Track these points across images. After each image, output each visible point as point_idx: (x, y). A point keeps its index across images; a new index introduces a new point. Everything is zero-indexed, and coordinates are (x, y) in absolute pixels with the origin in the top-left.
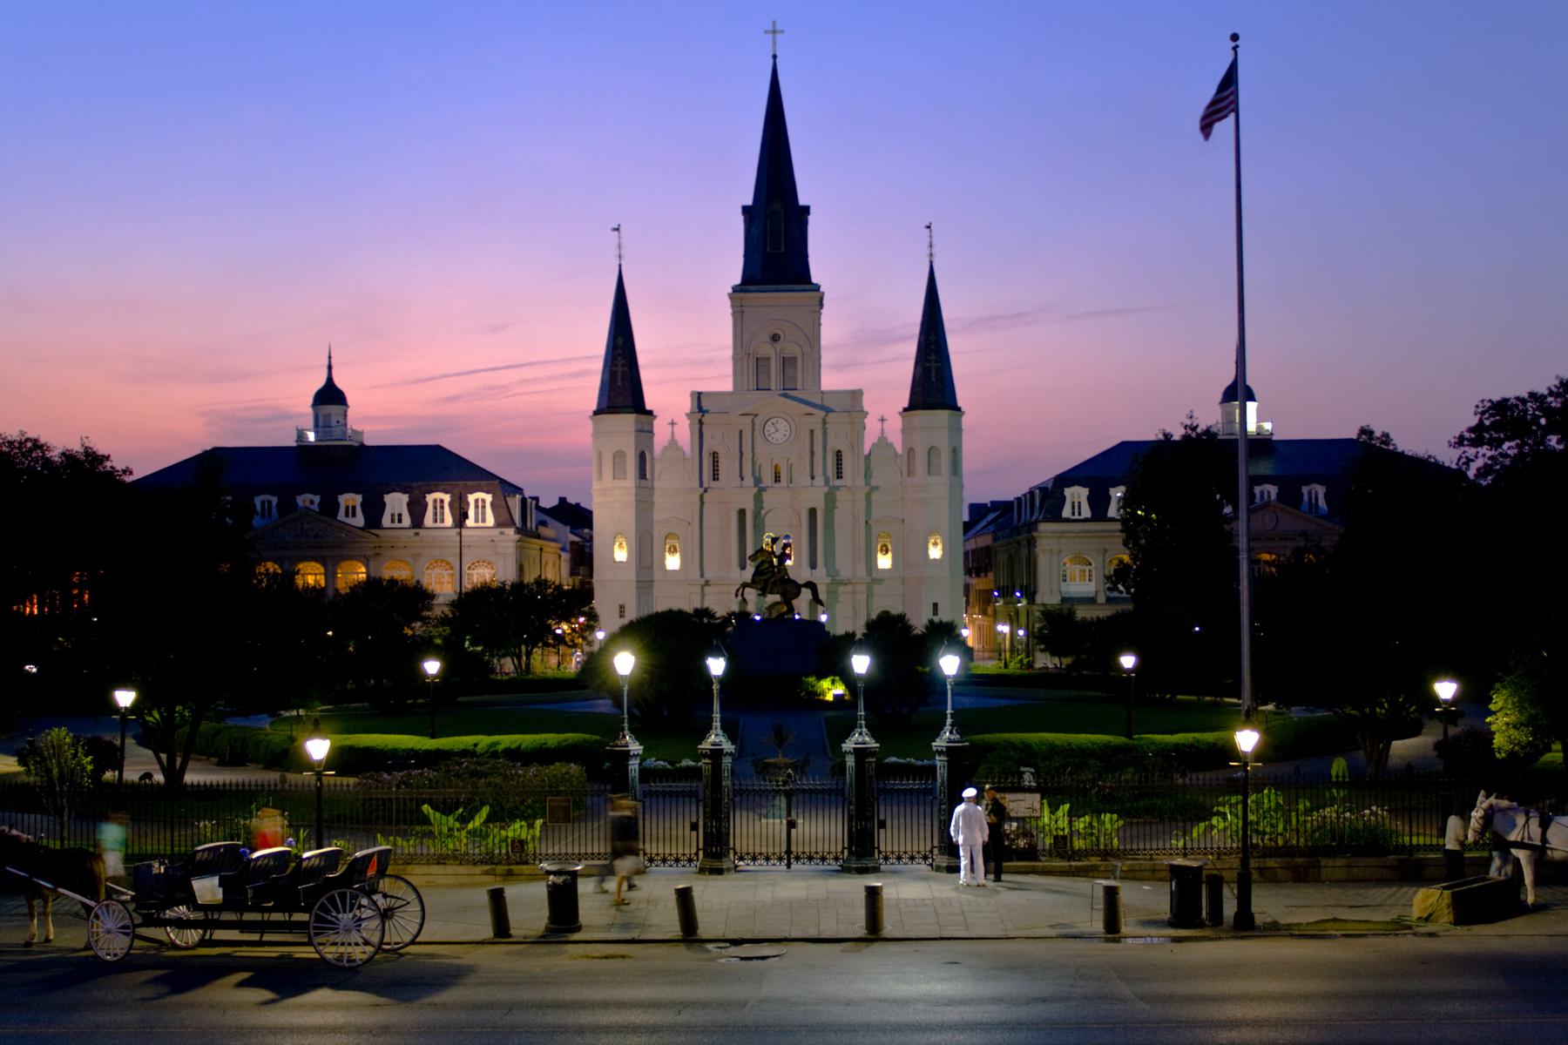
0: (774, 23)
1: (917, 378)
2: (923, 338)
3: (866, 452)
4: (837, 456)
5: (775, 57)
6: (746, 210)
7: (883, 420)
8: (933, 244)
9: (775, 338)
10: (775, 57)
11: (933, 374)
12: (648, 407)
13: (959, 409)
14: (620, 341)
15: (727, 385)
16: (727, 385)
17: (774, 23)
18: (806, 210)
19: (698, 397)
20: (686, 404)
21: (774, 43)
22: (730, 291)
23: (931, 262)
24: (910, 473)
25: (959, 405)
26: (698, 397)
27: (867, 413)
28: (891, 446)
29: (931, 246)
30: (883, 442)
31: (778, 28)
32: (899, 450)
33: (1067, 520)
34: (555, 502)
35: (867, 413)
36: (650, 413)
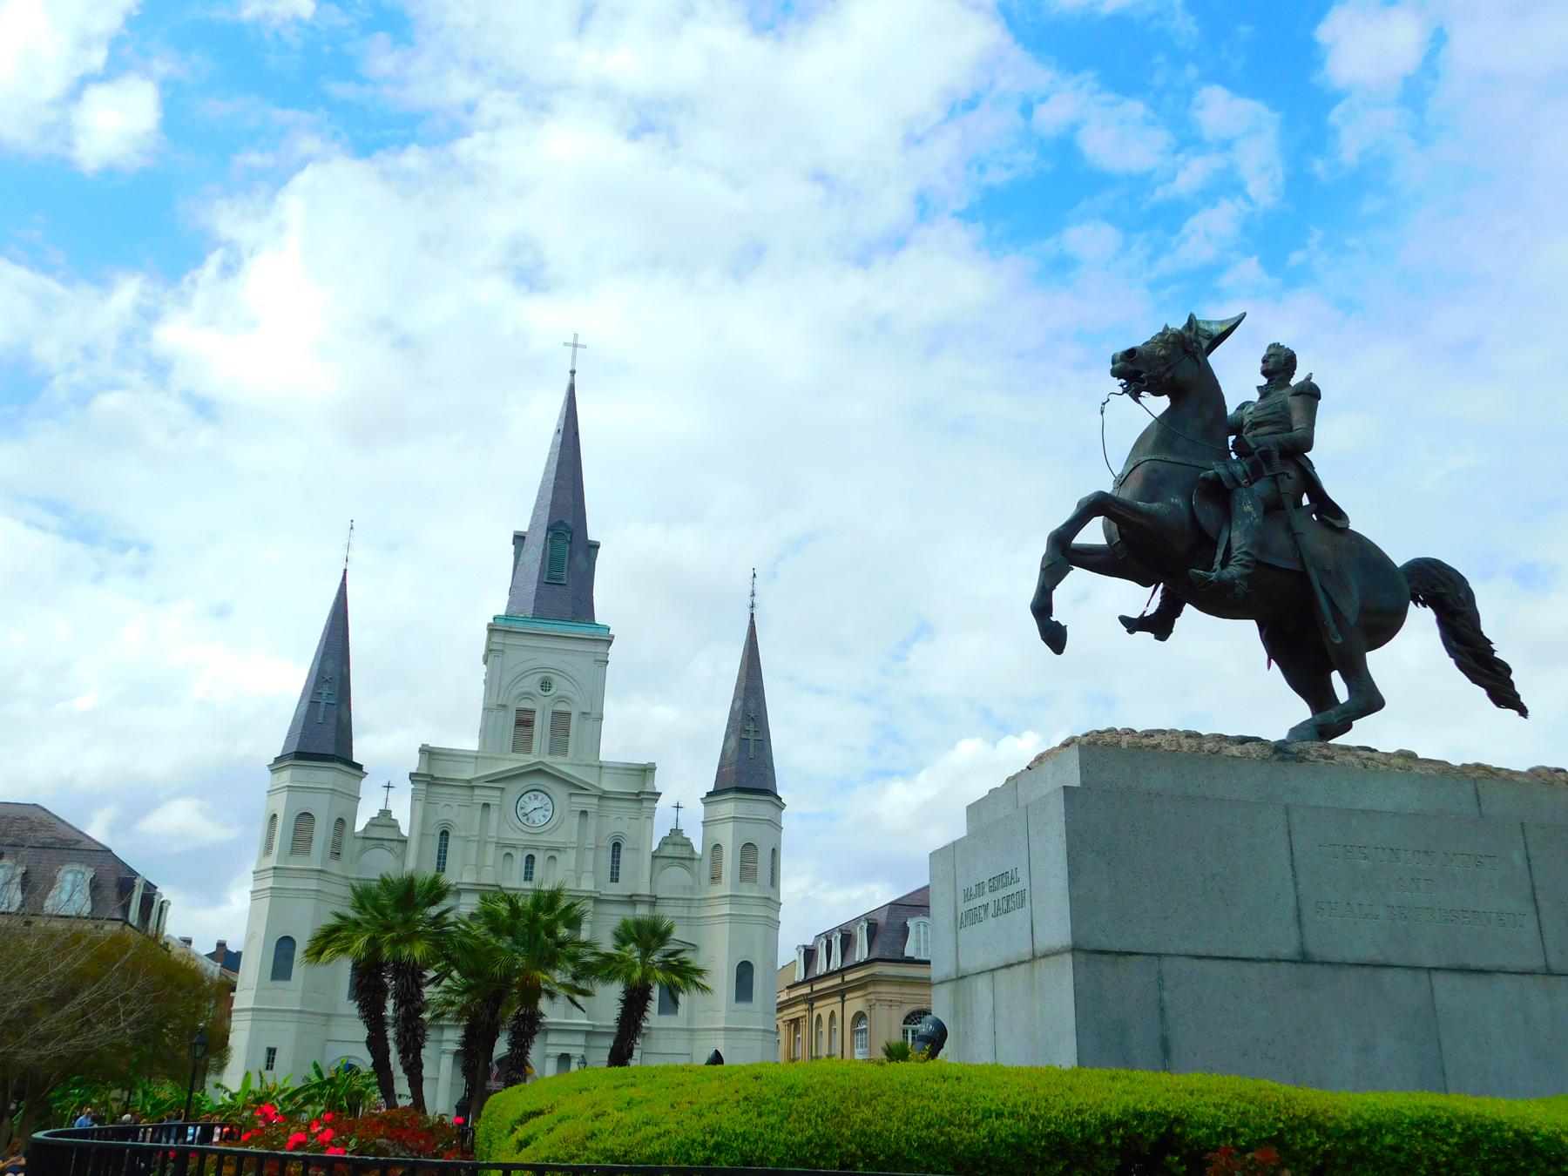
0: (576, 336)
1: (729, 752)
2: (739, 703)
3: (655, 847)
4: (613, 851)
5: (573, 373)
6: (519, 539)
7: (678, 807)
8: (756, 592)
9: (546, 685)
10: (573, 373)
11: (751, 750)
12: (355, 759)
13: (780, 799)
14: (330, 665)
15: (471, 744)
16: (471, 744)
17: (576, 336)
18: (596, 546)
19: (428, 753)
20: (413, 763)
21: (574, 357)
22: (492, 621)
23: (752, 615)
24: (715, 878)
25: (779, 794)
26: (428, 753)
27: (661, 794)
28: (687, 844)
29: (753, 595)
30: (676, 837)
31: (579, 342)
32: (698, 849)
33: (911, 961)
34: (213, 949)
35: (661, 794)
36: (359, 767)
